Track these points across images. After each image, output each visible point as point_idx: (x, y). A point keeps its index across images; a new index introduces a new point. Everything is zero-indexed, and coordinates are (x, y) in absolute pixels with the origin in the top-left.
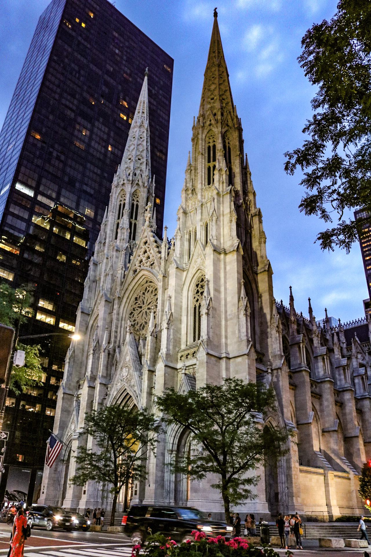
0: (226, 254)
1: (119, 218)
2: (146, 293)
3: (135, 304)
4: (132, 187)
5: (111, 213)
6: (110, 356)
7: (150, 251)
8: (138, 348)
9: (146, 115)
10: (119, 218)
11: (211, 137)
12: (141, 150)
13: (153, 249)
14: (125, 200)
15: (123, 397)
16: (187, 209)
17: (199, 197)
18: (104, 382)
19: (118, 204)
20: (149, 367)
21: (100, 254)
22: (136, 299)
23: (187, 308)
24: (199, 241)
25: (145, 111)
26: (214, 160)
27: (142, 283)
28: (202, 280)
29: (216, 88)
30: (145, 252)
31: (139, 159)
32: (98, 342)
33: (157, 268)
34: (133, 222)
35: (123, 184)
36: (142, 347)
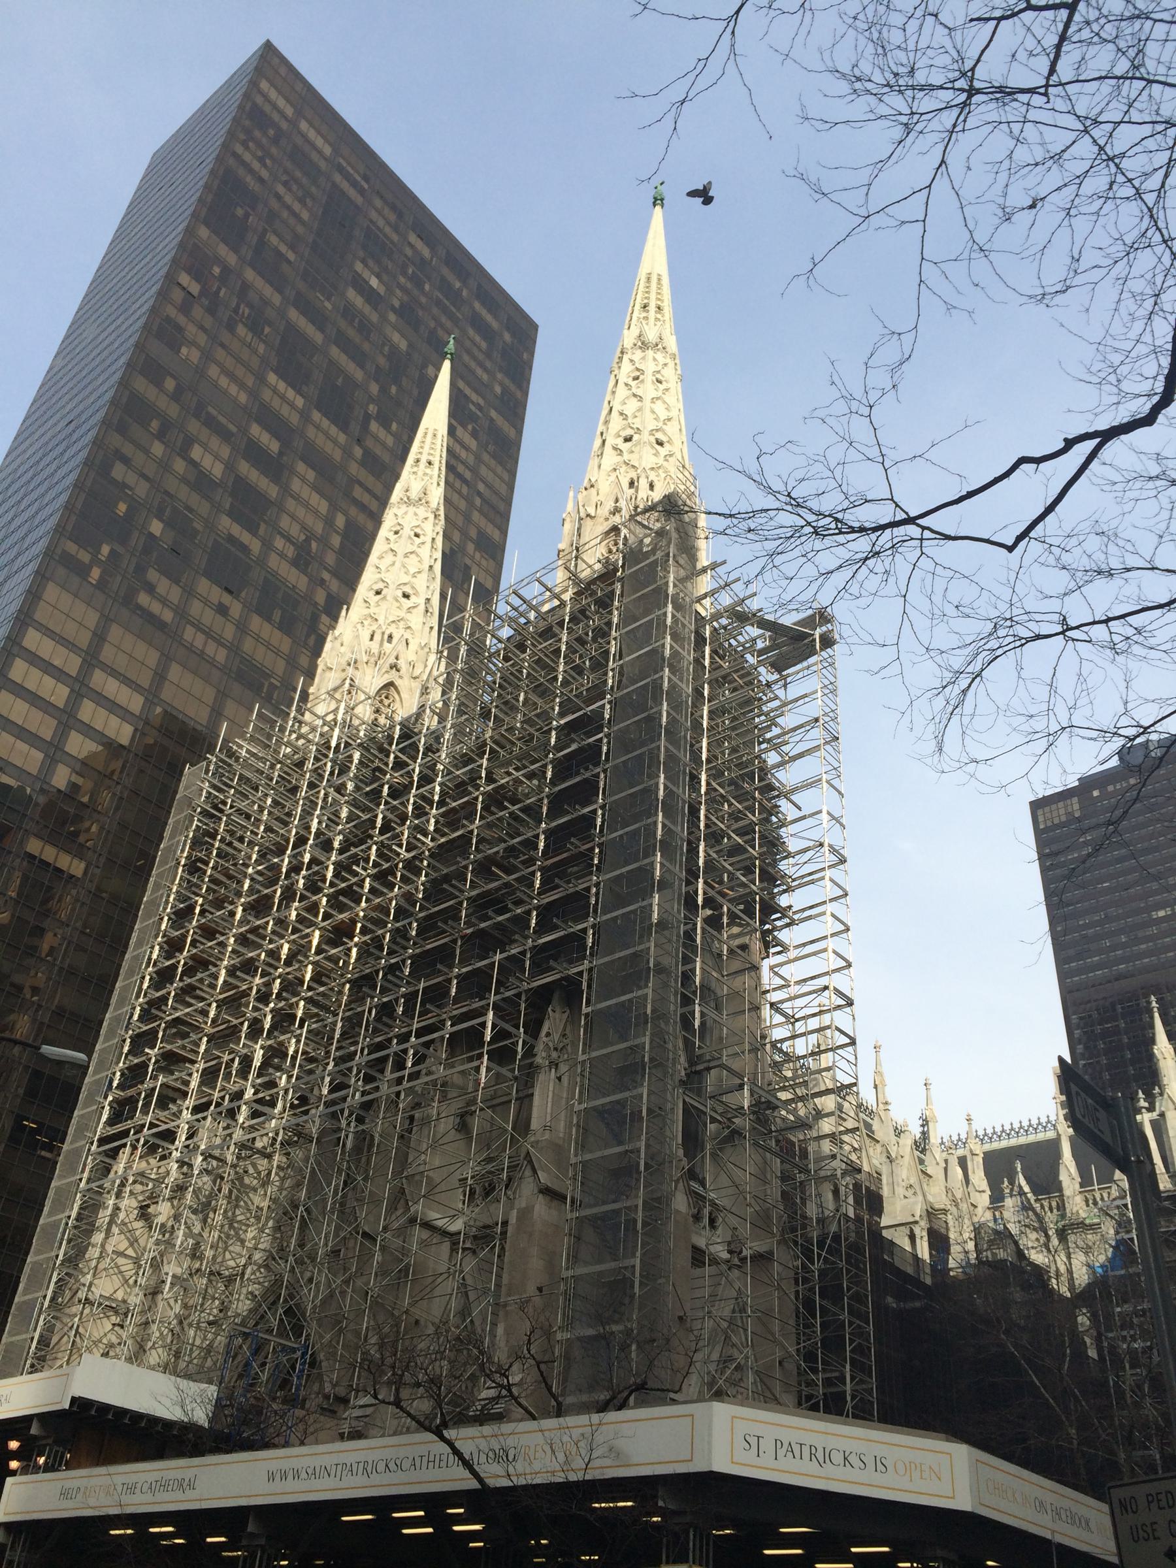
9: (436, 472)
12: (412, 570)
25: (436, 461)
29: (640, 409)
31: (406, 596)
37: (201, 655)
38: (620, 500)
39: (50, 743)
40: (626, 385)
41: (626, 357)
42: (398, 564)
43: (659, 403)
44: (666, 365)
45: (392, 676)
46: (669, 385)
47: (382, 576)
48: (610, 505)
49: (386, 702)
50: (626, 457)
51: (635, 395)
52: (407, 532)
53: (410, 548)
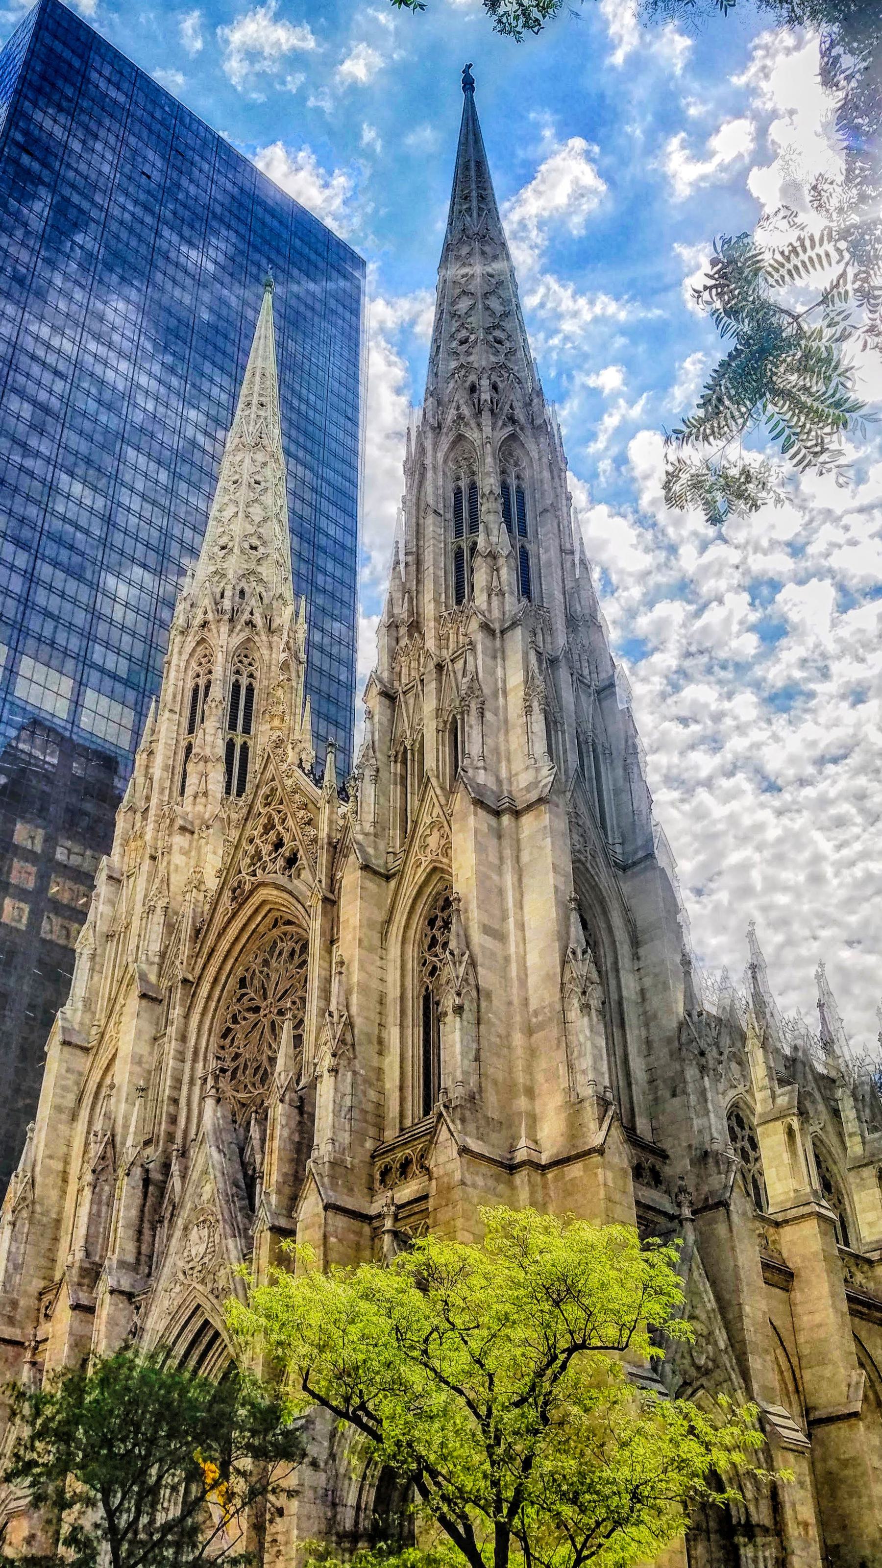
0: (517, 814)
1: (191, 731)
3: (239, 1000)
4: (231, 631)
5: (167, 714)
6: (151, 1188)
8: (242, 1150)
10: (191, 731)
12: (257, 519)
13: (293, 815)
14: (210, 672)
16: (396, 684)
17: (430, 644)
19: (190, 685)
20: (276, 1215)
21: (133, 845)
22: (242, 983)
24: (434, 781)
27: (261, 929)
28: (447, 903)
30: (269, 827)
33: (306, 874)
34: (239, 742)
35: (204, 625)
36: (257, 1147)
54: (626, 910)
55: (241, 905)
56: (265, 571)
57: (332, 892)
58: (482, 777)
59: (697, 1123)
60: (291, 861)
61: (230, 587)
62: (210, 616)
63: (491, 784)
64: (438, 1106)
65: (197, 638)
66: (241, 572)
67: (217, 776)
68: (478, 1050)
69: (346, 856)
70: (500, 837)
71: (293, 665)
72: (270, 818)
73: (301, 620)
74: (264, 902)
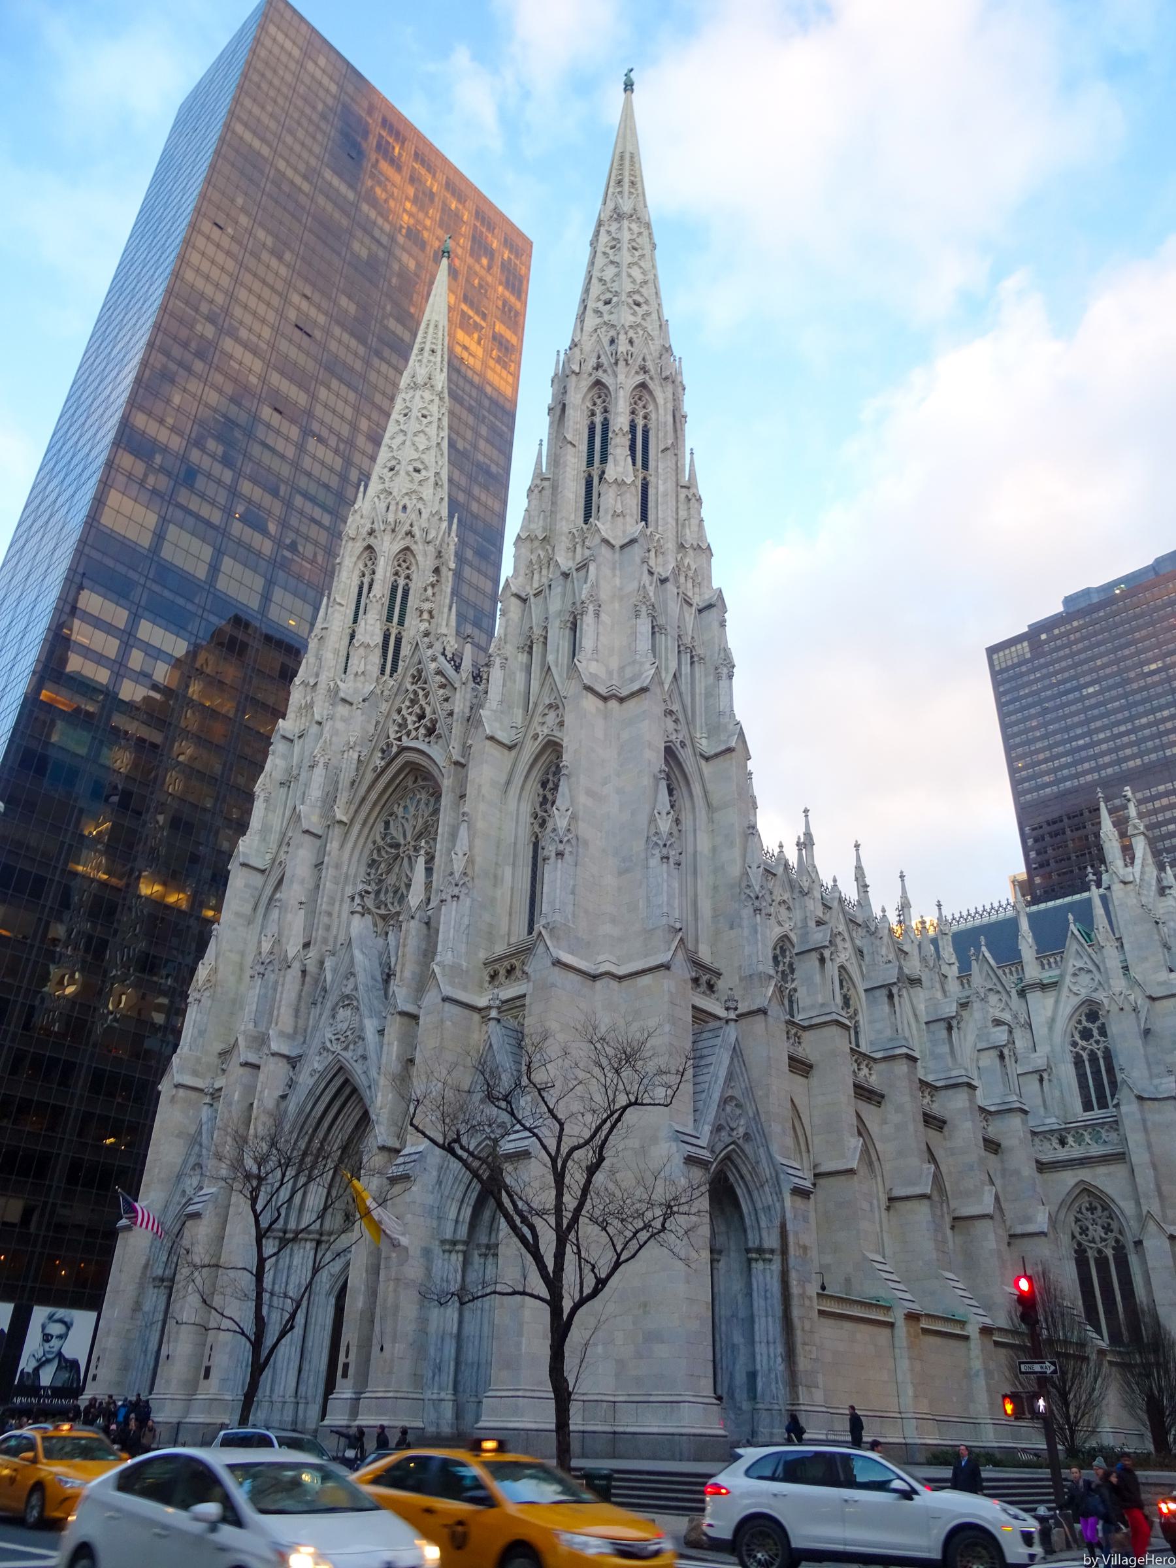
2: (412, 810)
6: (308, 979)
7: (426, 696)
9: (439, 359)
10: (355, 621)
11: (599, 401)
12: (421, 447)
15: (334, 1090)
18: (285, 1050)
19: (356, 582)
23: (515, 844)
24: (553, 668)
25: (439, 348)
26: (604, 460)
28: (558, 770)
29: (618, 275)
30: (414, 702)
31: (417, 471)
32: (278, 942)
34: (394, 632)
35: (371, 533)
37: (249, 549)
38: (603, 357)
39: (124, 631)
40: (604, 253)
41: (603, 230)
42: (408, 443)
43: (635, 268)
44: (640, 234)
45: (408, 542)
46: (644, 252)
47: (395, 454)
48: (592, 362)
49: (404, 565)
50: (606, 318)
51: (612, 262)
52: (415, 413)
53: (418, 427)
54: (706, 793)
55: (388, 764)
56: (427, 492)
57: (463, 757)
58: (594, 667)
59: (747, 950)
60: (430, 731)
61: (393, 503)
62: (376, 526)
63: (602, 673)
64: (538, 927)
65: (365, 544)
66: (404, 491)
67: (375, 658)
68: (574, 886)
69: (476, 728)
70: (605, 718)
71: (444, 570)
72: (415, 693)
73: (453, 534)
74: (407, 764)
